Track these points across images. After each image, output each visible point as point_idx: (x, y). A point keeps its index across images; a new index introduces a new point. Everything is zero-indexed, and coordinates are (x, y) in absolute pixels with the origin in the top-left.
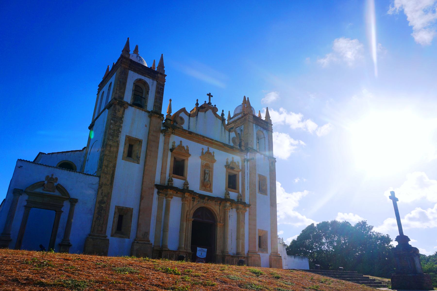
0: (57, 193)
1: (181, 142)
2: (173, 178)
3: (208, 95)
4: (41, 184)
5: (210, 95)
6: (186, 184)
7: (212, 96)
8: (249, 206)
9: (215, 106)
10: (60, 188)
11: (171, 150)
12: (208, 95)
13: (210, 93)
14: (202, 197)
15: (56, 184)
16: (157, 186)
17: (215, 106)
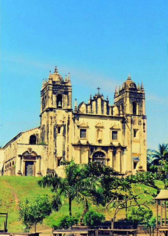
0: (33, 154)
1: (84, 121)
2: (80, 140)
3: (98, 89)
4: (27, 152)
5: (99, 89)
6: (88, 142)
7: (100, 89)
8: (125, 148)
9: (102, 94)
10: (33, 152)
11: (78, 126)
12: (98, 89)
13: (99, 88)
14: (96, 147)
15: (32, 151)
16: (73, 145)
17: (102, 94)
